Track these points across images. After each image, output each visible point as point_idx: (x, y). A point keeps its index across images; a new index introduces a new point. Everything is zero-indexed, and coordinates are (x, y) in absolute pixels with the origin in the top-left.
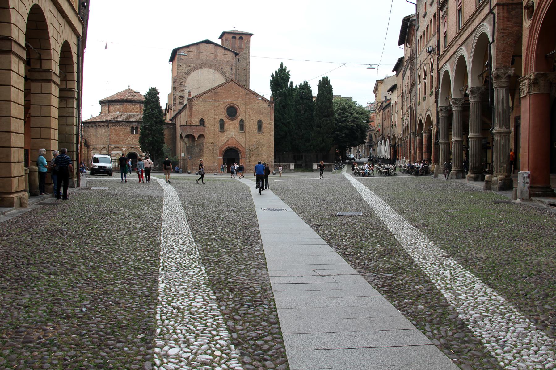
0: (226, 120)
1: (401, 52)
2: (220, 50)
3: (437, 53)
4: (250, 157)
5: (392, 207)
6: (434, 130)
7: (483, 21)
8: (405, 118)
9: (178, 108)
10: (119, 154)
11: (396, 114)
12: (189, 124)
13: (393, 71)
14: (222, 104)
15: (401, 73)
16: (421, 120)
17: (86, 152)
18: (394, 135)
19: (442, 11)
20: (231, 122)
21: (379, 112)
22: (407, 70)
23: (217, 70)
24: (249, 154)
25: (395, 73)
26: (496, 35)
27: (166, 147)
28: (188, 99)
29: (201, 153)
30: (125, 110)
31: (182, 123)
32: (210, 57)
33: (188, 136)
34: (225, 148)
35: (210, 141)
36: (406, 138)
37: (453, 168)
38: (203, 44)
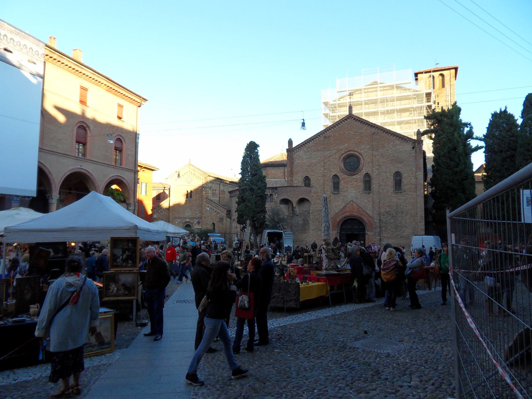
17: (228, 224)
20: (350, 178)
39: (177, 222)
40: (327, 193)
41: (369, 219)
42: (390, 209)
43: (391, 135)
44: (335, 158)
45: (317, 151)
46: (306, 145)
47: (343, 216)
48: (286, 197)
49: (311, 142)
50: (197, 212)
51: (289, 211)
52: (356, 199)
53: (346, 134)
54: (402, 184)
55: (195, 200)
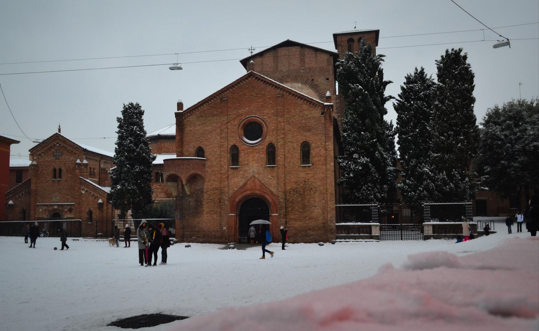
14: (234, 119)
24: (286, 208)
32: (294, 65)
35: (214, 186)
38: (282, 48)
39: (41, 210)
40: (225, 167)
41: (273, 198)
42: (297, 186)
43: (298, 98)
44: (233, 124)
45: (213, 116)
46: (199, 108)
47: (244, 194)
48: (172, 172)
49: (206, 104)
50: (68, 197)
51: (178, 190)
52: (259, 174)
53: (246, 95)
54: (310, 156)
55: (66, 181)
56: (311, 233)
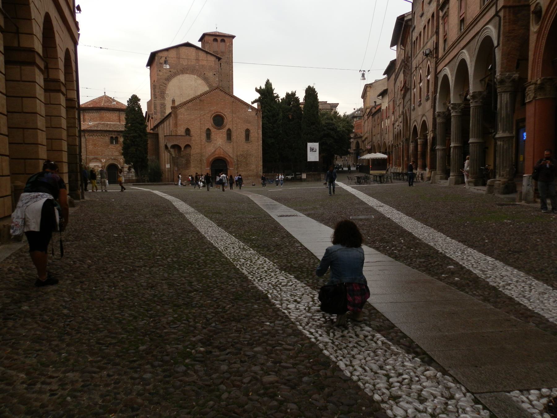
0: (213, 130)
1: (392, 54)
2: (202, 55)
3: (434, 56)
4: (238, 168)
5: (399, 211)
6: (430, 136)
7: (487, 24)
8: (397, 124)
9: (158, 117)
10: (98, 166)
11: (386, 121)
12: (175, 134)
13: (384, 74)
14: (208, 113)
15: (393, 76)
16: (415, 126)
18: (385, 143)
19: (442, 11)
20: (218, 131)
21: (368, 118)
22: (399, 73)
23: (199, 76)
24: (238, 165)
25: (385, 76)
26: (501, 38)
27: (150, 157)
28: (172, 108)
29: (187, 164)
30: (102, 119)
31: (165, 132)
33: (174, 147)
34: (212, 158)
35: (197, 152)
36: (398, 145)
37: (451, 174)
38: (183, 47)
56: (250, 178)
